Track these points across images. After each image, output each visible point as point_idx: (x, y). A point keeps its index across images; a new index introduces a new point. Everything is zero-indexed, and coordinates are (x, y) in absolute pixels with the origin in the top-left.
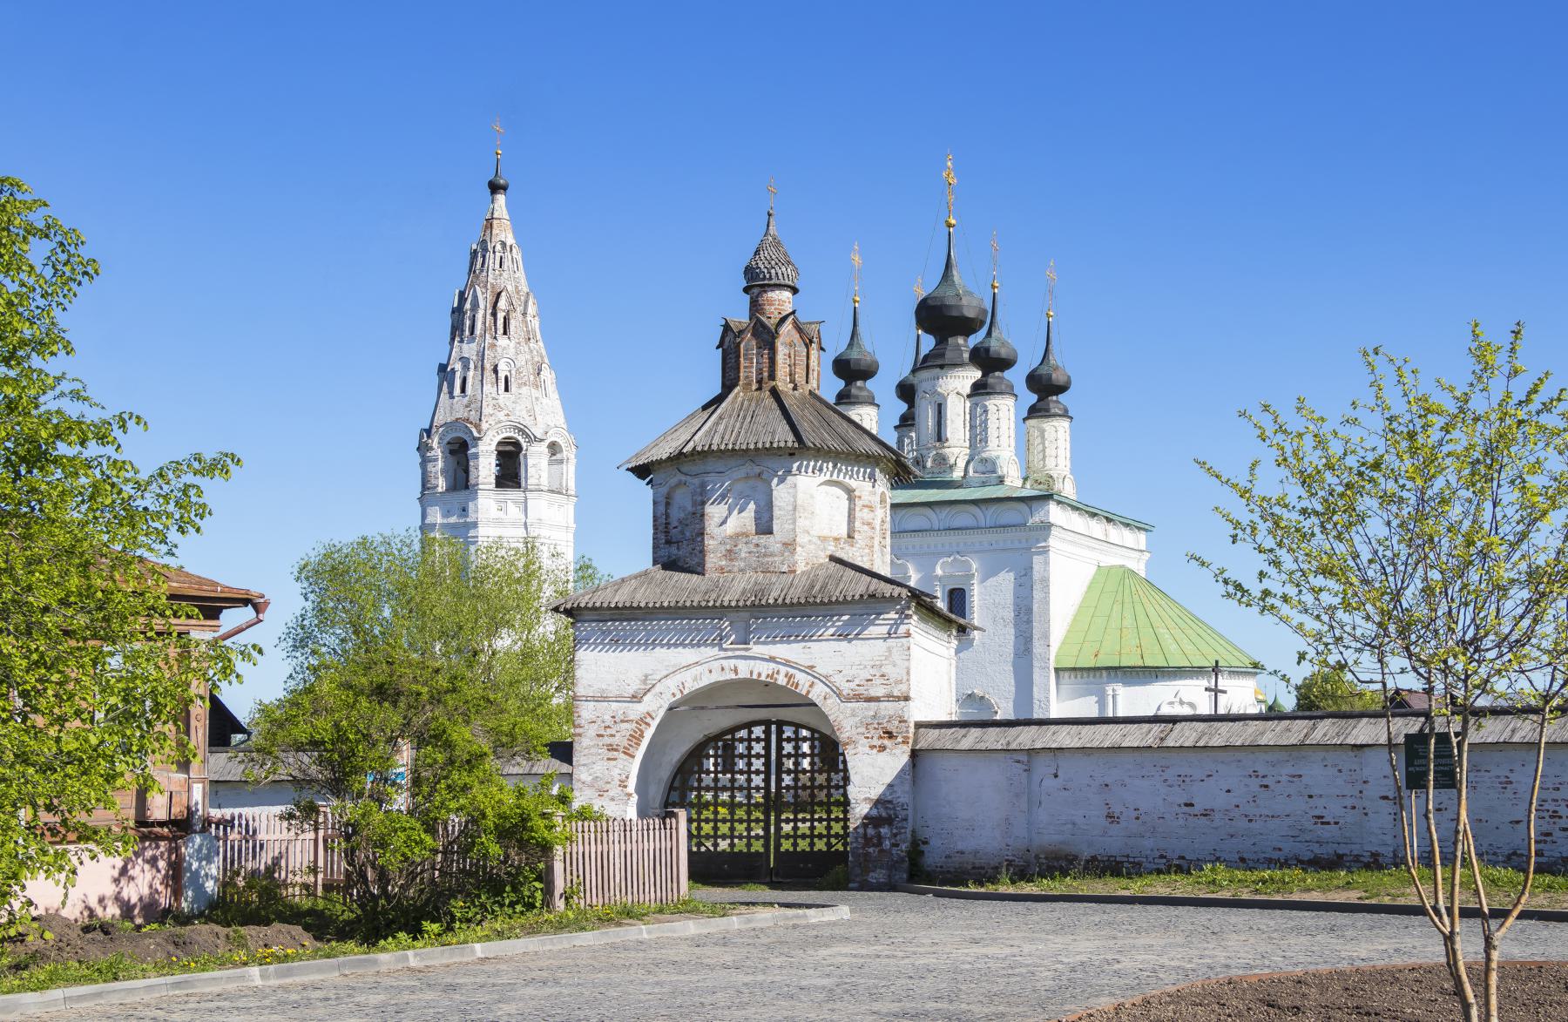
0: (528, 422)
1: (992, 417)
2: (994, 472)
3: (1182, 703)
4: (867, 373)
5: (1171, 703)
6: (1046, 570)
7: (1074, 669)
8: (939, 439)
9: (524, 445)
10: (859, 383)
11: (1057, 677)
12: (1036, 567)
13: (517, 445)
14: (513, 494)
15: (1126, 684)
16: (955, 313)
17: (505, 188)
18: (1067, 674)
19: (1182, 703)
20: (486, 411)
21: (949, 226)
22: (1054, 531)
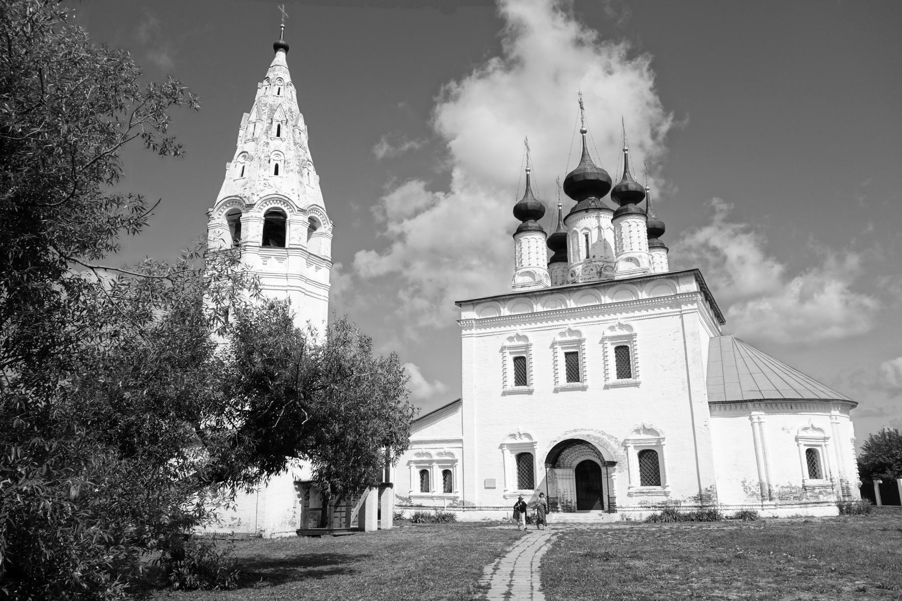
3: (814, 428)
5: (806, 429)
7: (723, 402)
9: (288, 214)
13: (283, 215)
17: (286, 48)
19: (814, 428)
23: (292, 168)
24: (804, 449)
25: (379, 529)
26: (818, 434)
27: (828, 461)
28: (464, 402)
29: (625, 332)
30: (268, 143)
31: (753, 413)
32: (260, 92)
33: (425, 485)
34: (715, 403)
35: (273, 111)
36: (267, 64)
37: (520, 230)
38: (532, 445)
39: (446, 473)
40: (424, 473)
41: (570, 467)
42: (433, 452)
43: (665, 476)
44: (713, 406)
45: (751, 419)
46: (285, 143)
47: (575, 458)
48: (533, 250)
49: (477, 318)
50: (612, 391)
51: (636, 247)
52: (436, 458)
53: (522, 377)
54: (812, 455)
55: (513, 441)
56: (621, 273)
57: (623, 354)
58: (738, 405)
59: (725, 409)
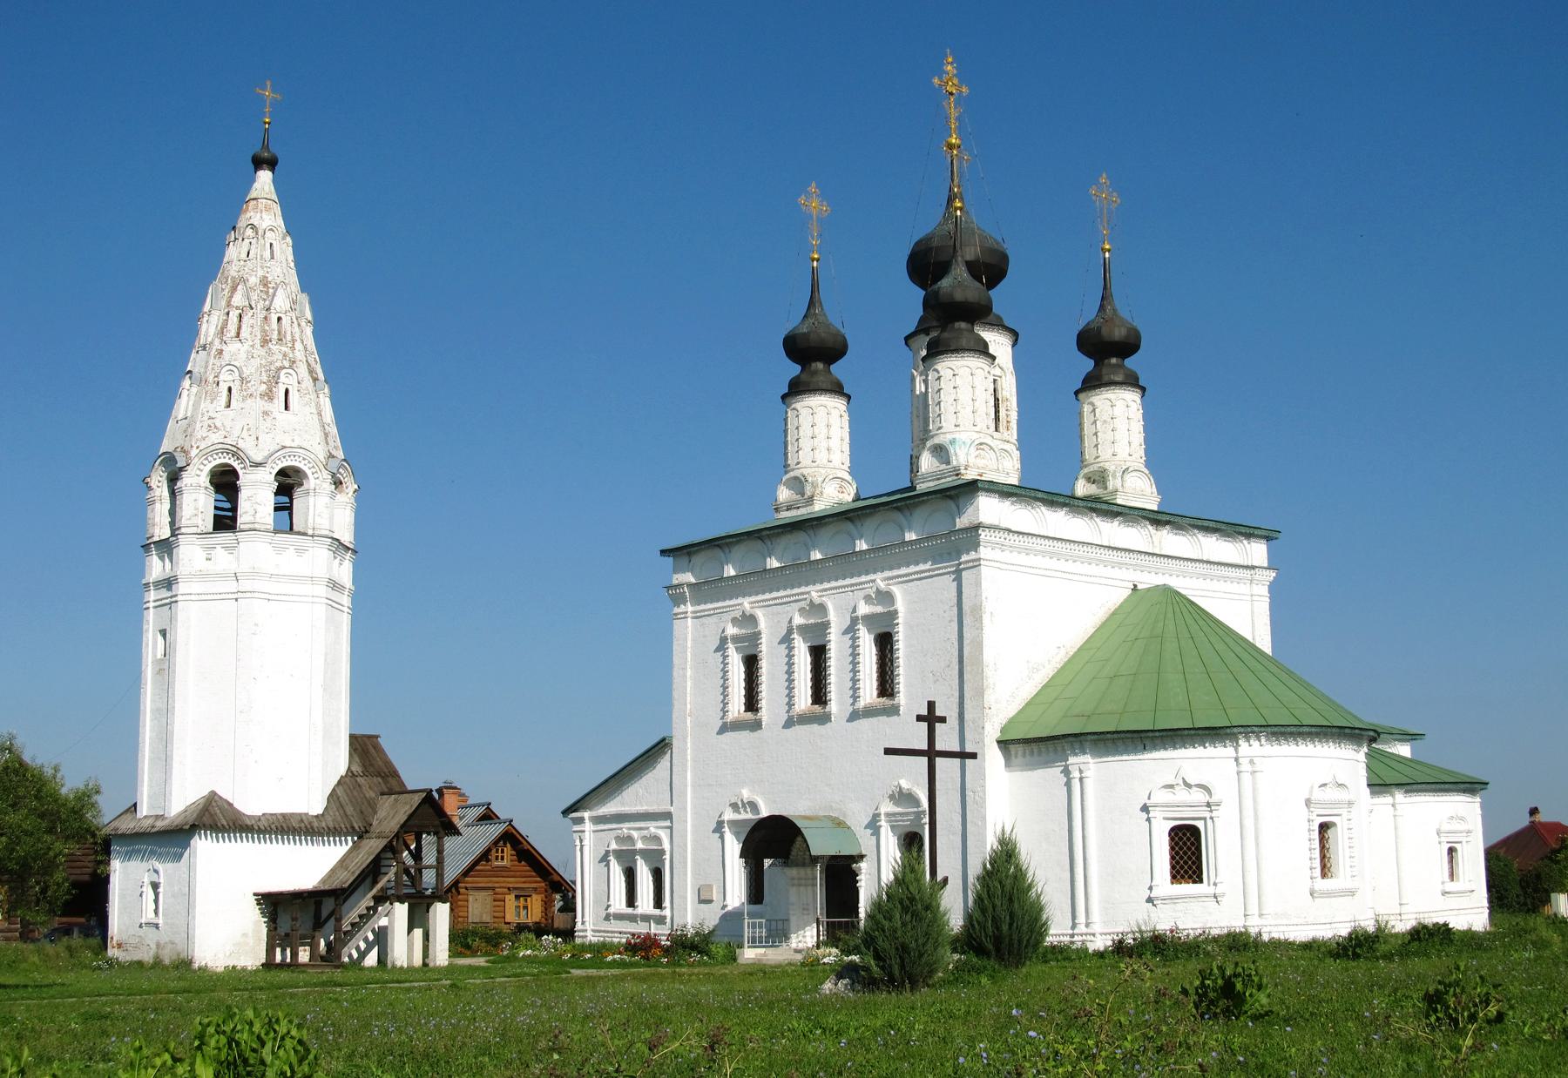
0: (247, 445)
2: (948, 463)
3: (1188, 786)
6: (978, 595)
14: (225, 537)
17: (272, 164)
20: (199, 433)
21: (951, 147)
22: (984, 535)
23: (252, 390)
25: (425, 964)
26: (1198, 796)
28: (675, 743)
30: (220, 352)
31: (1072, 760)
32: (233, 252)
33: (631, 900)
35: (234, 289)
36: (239, 199)
39: (658, 875)
40: (630, 875)
42: (635, 834)
45: (1066, 772)
46: (246, 346)
48: (821, 430)
49: (693, 580)
50: (864, 724)
51: (948, 422)
52: (640, 845)
55: (737, 817)
56: (925, 479)
59: (1032, 753)
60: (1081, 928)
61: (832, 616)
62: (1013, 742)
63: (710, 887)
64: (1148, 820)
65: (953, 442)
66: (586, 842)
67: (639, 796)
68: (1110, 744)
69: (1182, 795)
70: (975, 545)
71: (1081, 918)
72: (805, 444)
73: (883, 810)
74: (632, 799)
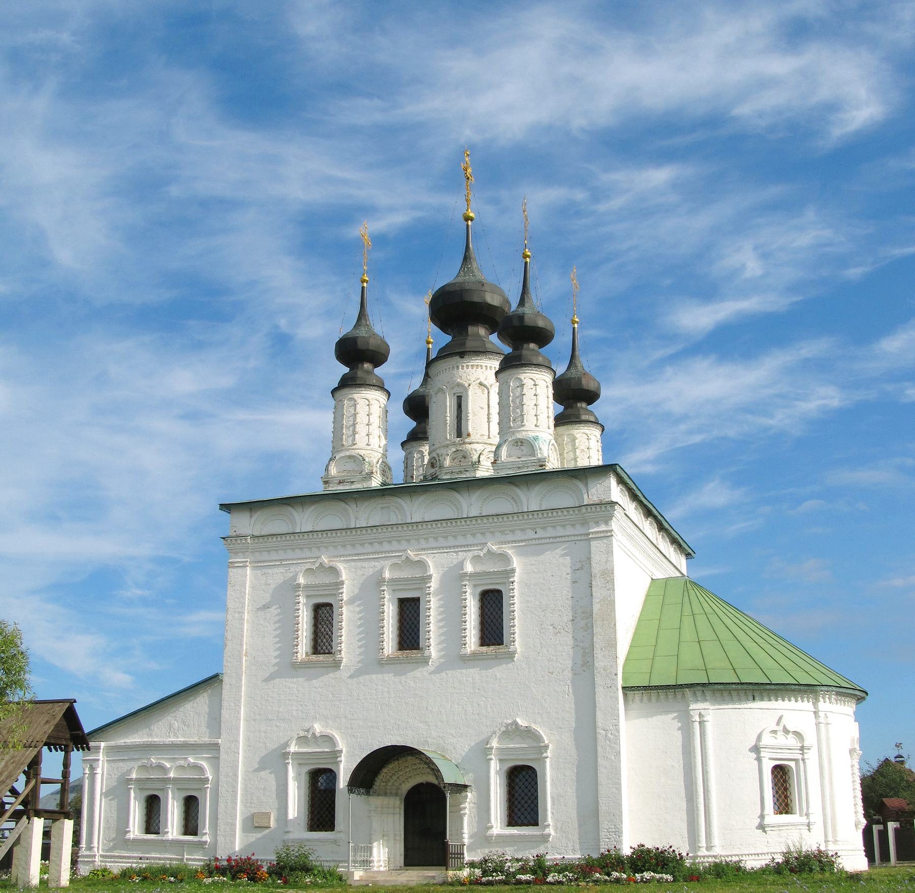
1: (528, 392)
2: (533, 454)
3: (786, 731)
4: (378, 357)
7: (645, 688)
8: (459, 435)
10: (367, 366)
11: (625, 695)
12: (595, 558)
15: (715, 701)
16: (476, 299)
18: (638, 695)
24: (768, 766)
26: (792, 741)
27: (809, 785)
28: (226, 679)
29: (327, 579)
34: (632, 688)
37: (347, 383)
38: (336, 754)
39: (191, 805)
40: (153, 805)
41: (397, 795)
43: (546, 810)
44: (630, 693)
47: (408, 778)
53: (410, 635)
54: (781, 774)
57: (492, 604)
58: (670, 693)
59: (650, 700)
60: (703, 852)
61: (432, 571)
62: (638, 688)
63: (267, 815)
64: (759, 759)
65: (536, 439)
66: (99, 771)
67: (185, 724)
68: (725, 694)
69: (781, 740)
70: (608, 519)
71: (703, 843)
72: (361, 429)
73: (494, 744)
74: (160, 731)
